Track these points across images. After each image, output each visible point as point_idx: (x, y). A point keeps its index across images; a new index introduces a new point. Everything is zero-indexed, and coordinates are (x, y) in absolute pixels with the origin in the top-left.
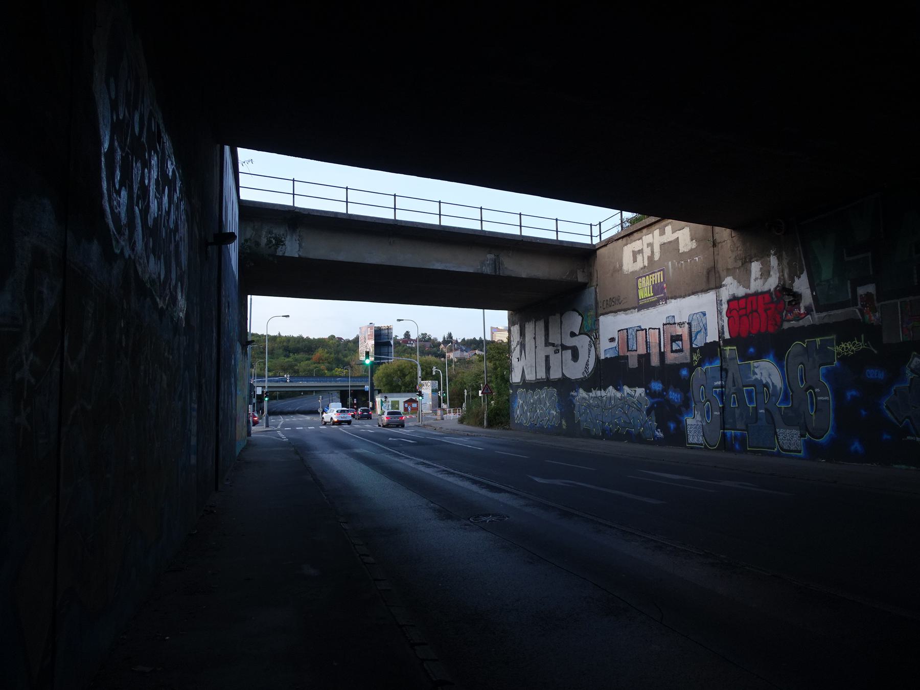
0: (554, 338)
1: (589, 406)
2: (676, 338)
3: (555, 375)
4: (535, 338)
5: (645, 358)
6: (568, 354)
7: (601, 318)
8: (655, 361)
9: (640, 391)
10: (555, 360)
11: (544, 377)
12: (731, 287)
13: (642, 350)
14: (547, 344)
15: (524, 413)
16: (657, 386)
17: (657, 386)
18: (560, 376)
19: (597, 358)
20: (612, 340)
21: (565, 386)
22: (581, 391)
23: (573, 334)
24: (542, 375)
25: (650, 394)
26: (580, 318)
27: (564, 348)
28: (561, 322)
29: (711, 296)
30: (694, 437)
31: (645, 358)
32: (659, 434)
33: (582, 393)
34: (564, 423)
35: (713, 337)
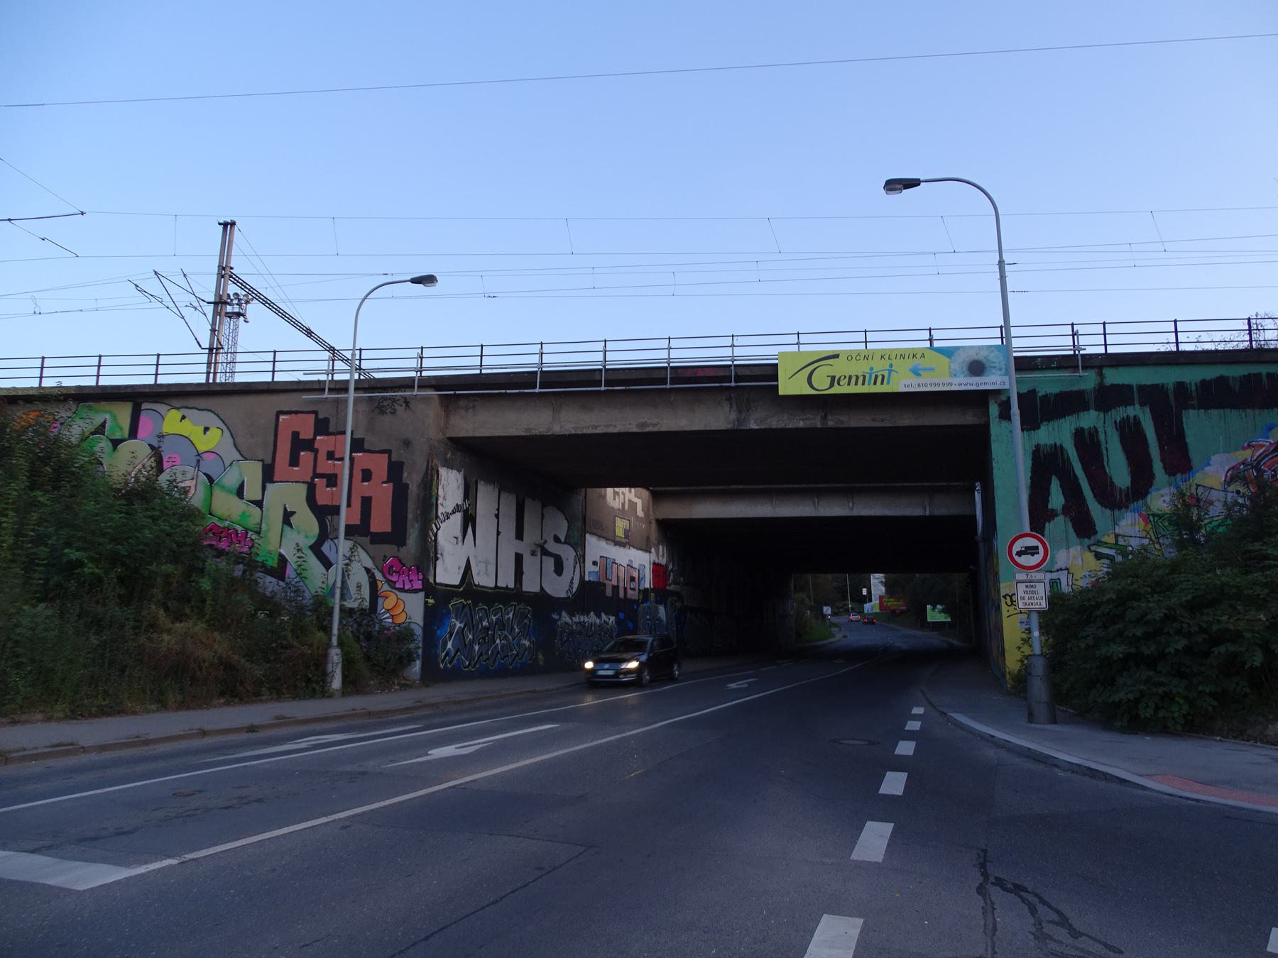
1: (571, 633)
2: (632, 579)
3: (530, 586)
4: (497, 516)
5: (616, 588)
6: (549, 563)
7: (587, 536)
9: (612, 618)
10: (530, 565)
11: (512, 585)
12: (653, 557)
14: (519, 535)
15: (463, 646)
16: (622, 615)
17: (622, 615)
18: (537, 589)
19: (582, 577)
20: (595, 563)
21: (542, 603)
22: (564, 614)
23: (557, 539)
24: (507, 580)
25: (618, 621)
26: (565, 524)
27: (545, 552)
29: (646, 555)
31: (616, 588)
33: (565, 618)
34: (540, 656)
35: (647, 586)
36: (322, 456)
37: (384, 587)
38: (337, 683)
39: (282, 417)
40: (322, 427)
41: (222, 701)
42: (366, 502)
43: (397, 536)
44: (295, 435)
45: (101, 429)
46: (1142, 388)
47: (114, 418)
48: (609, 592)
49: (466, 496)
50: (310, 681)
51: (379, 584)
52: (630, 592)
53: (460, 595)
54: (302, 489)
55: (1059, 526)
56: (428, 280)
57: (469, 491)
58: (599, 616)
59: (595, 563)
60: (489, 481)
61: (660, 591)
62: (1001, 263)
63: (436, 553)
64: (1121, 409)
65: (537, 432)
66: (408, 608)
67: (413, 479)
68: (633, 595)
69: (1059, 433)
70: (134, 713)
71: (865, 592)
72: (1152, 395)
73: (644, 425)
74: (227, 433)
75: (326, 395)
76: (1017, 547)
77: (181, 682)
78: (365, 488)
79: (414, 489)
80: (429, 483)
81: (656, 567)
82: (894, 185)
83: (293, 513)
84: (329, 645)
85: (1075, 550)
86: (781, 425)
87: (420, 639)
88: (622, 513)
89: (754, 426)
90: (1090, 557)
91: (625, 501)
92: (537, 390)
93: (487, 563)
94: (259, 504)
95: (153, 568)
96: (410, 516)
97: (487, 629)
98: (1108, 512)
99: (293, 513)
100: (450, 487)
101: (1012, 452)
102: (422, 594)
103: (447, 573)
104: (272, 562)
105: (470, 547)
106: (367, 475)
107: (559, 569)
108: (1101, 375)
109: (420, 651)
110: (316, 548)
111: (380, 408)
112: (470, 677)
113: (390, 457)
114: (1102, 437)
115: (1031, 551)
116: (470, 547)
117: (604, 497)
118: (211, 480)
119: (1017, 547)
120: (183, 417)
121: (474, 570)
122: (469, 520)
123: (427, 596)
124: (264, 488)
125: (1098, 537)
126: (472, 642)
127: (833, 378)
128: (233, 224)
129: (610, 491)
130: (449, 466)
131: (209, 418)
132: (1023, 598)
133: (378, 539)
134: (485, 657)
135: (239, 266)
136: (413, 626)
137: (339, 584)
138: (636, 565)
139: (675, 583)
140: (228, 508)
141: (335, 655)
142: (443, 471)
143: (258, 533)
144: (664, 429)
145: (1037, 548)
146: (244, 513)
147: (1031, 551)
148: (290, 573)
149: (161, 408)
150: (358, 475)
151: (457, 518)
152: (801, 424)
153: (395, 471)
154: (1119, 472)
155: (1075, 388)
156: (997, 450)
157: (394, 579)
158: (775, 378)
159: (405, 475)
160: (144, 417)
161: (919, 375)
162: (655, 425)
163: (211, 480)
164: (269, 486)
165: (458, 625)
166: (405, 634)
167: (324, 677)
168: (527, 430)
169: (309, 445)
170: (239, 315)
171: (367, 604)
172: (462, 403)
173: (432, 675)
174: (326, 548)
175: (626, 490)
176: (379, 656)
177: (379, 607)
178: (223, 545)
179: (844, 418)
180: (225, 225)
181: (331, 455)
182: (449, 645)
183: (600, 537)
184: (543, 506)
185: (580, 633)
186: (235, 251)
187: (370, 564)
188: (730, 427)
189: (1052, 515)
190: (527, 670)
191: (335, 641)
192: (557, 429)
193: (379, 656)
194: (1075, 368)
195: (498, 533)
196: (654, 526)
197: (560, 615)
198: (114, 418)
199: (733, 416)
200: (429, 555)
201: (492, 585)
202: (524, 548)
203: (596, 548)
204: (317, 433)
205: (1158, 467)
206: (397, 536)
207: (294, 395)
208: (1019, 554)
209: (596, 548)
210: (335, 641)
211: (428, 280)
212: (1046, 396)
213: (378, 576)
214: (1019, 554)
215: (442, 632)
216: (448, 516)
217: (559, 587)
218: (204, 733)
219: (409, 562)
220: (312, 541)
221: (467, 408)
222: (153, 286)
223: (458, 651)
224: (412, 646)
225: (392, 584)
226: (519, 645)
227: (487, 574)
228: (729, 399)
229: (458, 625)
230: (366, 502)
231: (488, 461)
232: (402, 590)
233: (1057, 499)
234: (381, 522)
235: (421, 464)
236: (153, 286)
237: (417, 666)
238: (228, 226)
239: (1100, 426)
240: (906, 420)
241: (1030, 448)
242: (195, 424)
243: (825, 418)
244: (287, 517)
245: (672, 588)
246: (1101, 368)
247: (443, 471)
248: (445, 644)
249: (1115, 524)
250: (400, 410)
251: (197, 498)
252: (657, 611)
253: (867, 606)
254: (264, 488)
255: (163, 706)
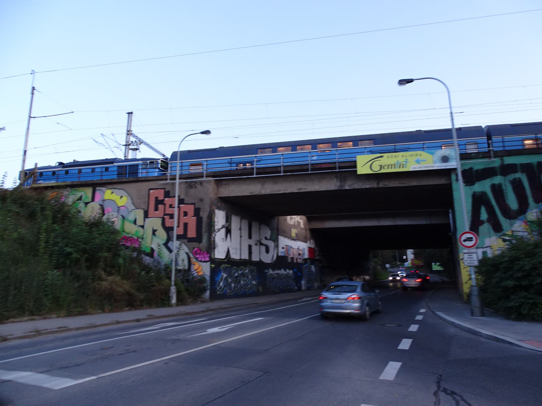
0: (255, 237)
1: (274, 278)
2: (300, 254)
3: (255, 258)
4: (240, 229)
6: (263, 248)
8: (295, 261)
9: (291, 272)
10: (255, 249)
13: (292, 256)
14: (250, 237)
15: (227, 284)
16: (295, 270)
17: (295, 270)
19: (278, 254)
20: (283, 248)
21: (261, 266)
22: (270, 270)
23: (266, 238)
24: (245, 256)
25: (294, 273)
27: (261, 244)
28: (260, 229)
30: (303, 288)
31: (292, 258)
32: (296, 288)
33: (271, 271)
36: (167, 206)
37: (193, 260)
38: (174, 301)
39: (151, 191)
40: (167, 194)
41: (127, 309)
42: (186, 225)
43: (198, 239)
44: (157, 198)
45: (80, 199)
46: (522, 165)
47: (86, 194)
48: (289, 260)
49: (227, 221)
50: (163, 300)
51: (192, 259)
52: (299, 260)
53: (225, 263)
54: (160, 221)
55: (485, 228)
56: (207, 132)
57: (228, 219)
58: (285, 271)
59: (283, 248)
60: (236, 214)
61: (312, 259)
62: (451, 113)
63: (214, 245)
64: (513, 174)
65: (254, 194)
66: (203, 269)
67: (204, 215)
68: (300, 261)
69: (484, 186)
70: (92, 314)
71: (405, 257)
72: (526, 168)
73: (300, 189)
74: (129, 199)
75: (168, 181)
76: (464, 237)
77: (111, 301)
78: (184, 219)
79: (205, 219)
80: (211, 216)
81: (310, 249)
82: (403, 82)
83: (156, 230)
84: (170, 285)
85: (494, 238)
86: (359, 187)
87: (209, 281)
88: (294, 226)
89: (347, 188)
90: (500, 241)
91: (296, 221)
92: (254, 176)
93: (236, 249)
94: (143, 227)
95: (100, 254)
96: (204, 230)
97: (237, 277)
98: (508, 221)
99: (156, 230)
100: (220, 218)
101: (462, 196)
102: (209, 263)
103: (220, 254)
104: (148, 251)
105: (229, 243)
106: (186, 214)
107: (267, 251)
108: (502, 160)
109: (209, 287)
110: (166, 244)
111: (190, 186)
112: (231, 297)
113: (195, 206)
114: (504, 187)
115: (470, 239)
116: (229, 243)
117: (286, 220)
118: (124, 218)
119: (464, 237)
120: (112, 193)
121: (231, 252)
122: (228, 231)
123: (211, 264)
124: (144, 220)
125: (504, 232)
126: (231, 282)
127: (381, 166)
128: (132, 113)
129: (288, 217)
130: (219, 209)
131: (122, 192)
132: (467, 261)
133: (191, 240)
134: (236, 289)
135: (134, 130)
136: (206, 276)
137: (174, 260)
138: (301, 248)
139: (318, 255)
140: (131, 229)
141: (173, 289)
142: (217, 211)
143: (143, 239)
144: (308, 190)
145: (472, 238)
146: (137, 231)
147: (470, 239)
148: (155, 255)
149: (103, 189)
150: (182, 214)
151: (223, 231)
152: (368, 186)
153: (197, 212)
154: (513, 202)
155: (490, 166)
156: (455, 194)
157: (197, 256)
158: (355, 167)
159: (201, 213)
160: (98, 193)
161: (419, 163)
162: (305, 189)
163: (124, 218)
164: (147, 220)
165: (225, 275)
166: (202, 280)
167: (169, 298)
168: (252, 193)
169: (162, 202)
170: (137, 149)
171: (187, 267)
172: (224, 182)
173: (214, 297)
174: (170, 244)
175: (295, 216)
176: (191, 289)
177: (192, 268)
178: (128, 244)
179: (387, 183)
180: (129, 113)
181: (171, 206)
182: (221, 284)
183: (285, 237)
184: (260, 225)
185: (277, 278)
186: (133, 124)
187: (187, 251)
188: (336, 188)
189: (482, 223)
190: (255, 294)
191: (173, 283)
192: (263, 192)
193: (191, 289)
194: (490, 157)
195: (241, 236)
196: (308, 231)
197: (268, 270)
198: (86, 194)
199: (338, 184)
200: (211, 246)
201: (239, 258)
202: (252, 242)
203: (283, 241)
204: (165, 197)
205: (531, 200)
206: (198, 239)
207: (157, 182)
208: (465, 241)
209: (283, 241)
210: (173, 283)
211: (207, 132)
212: (477, 171)
213: (191, 255)
214: (465, 241)
215: (218, 279)
216: (219, 230)
217: (268, 259)
218: (118, 322)
219: (204, 250)
220: (164, 242)
221: (226, 185)
222: (101, 140)
223: (225, 286)
224: (205, 285)
225: (197, 259)
226: (251, 283)
227: (236, 254)
228: (336, 177)
229: (225, 275)
230: (186, 225)
231: (235, 206)
232: (201, 261)
233: (484, 216)
234: (192, 233)
235: (207, 209)
236: (101, 140)
237: (208, 293)
238: (130, 113)
239: (502, 182)
240: (414, 183)
241: (470, 193)
242: (118, 195)
243: (378, 183)
244: (154, 231)
245: (316, 258)
246: (502, 157)
247: (217, 211)
248: (219, 284)
249: (512, 225)
250: (199, 186)
251: (118, 226)
252: (311, 268)
253: (406, 264)
254: (144, 220)
255: (104, 311)
